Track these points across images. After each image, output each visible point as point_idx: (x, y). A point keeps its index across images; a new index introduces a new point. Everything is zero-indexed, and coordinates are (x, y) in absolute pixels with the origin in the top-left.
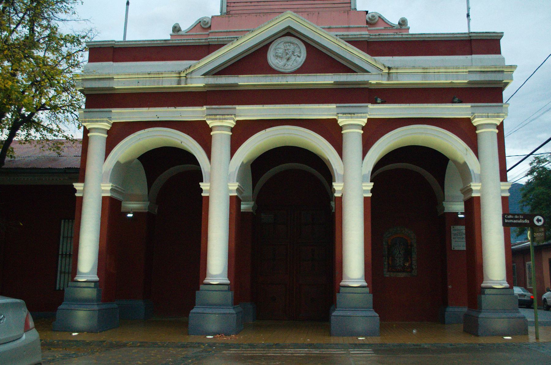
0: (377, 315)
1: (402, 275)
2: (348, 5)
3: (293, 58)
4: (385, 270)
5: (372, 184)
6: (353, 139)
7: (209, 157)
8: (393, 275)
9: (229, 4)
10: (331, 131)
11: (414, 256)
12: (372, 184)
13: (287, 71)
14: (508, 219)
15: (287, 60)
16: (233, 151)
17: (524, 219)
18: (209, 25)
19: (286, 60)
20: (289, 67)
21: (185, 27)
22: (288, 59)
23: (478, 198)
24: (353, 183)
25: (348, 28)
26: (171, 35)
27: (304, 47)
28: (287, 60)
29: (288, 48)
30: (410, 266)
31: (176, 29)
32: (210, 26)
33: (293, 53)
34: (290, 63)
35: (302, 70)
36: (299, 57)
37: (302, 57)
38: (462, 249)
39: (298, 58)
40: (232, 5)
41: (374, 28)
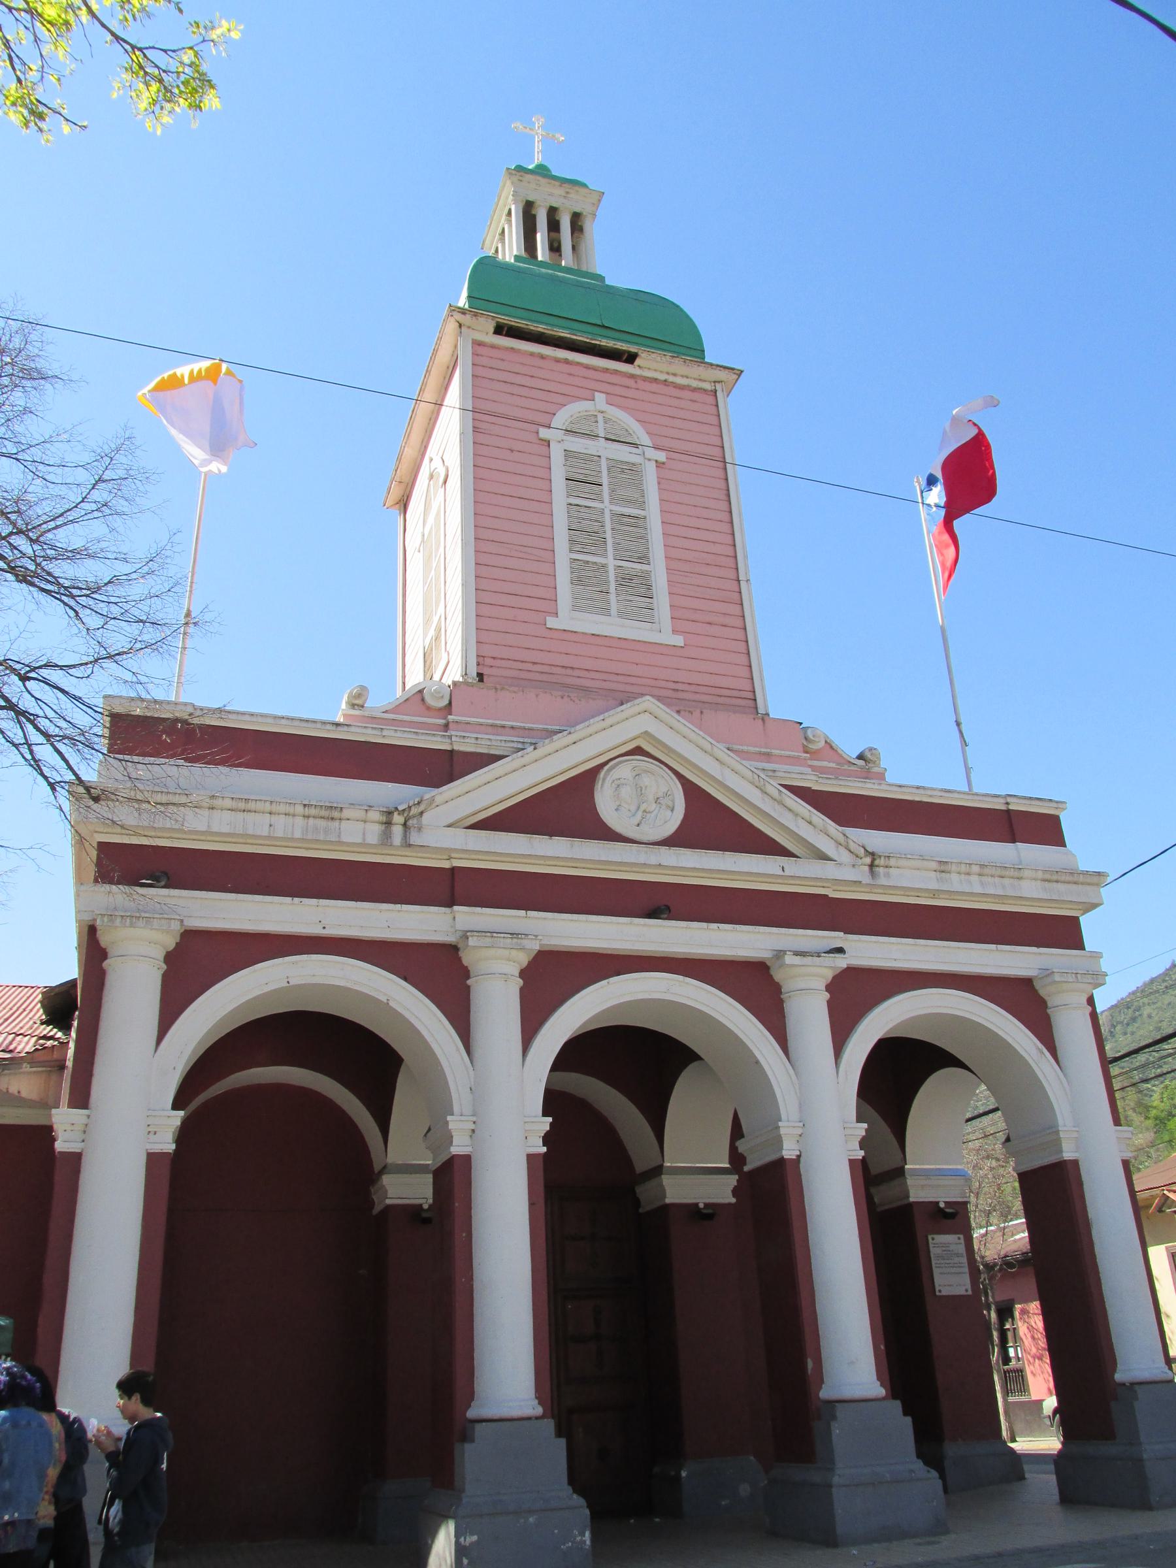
6: (810, 1012)
13: (645, 839)
21: (377, 701)
23: (1075, 1163)
25: (768, 755)
26: (345, 715)
31: (357, 701)
35: (671, 842)
38: (963, 1292)
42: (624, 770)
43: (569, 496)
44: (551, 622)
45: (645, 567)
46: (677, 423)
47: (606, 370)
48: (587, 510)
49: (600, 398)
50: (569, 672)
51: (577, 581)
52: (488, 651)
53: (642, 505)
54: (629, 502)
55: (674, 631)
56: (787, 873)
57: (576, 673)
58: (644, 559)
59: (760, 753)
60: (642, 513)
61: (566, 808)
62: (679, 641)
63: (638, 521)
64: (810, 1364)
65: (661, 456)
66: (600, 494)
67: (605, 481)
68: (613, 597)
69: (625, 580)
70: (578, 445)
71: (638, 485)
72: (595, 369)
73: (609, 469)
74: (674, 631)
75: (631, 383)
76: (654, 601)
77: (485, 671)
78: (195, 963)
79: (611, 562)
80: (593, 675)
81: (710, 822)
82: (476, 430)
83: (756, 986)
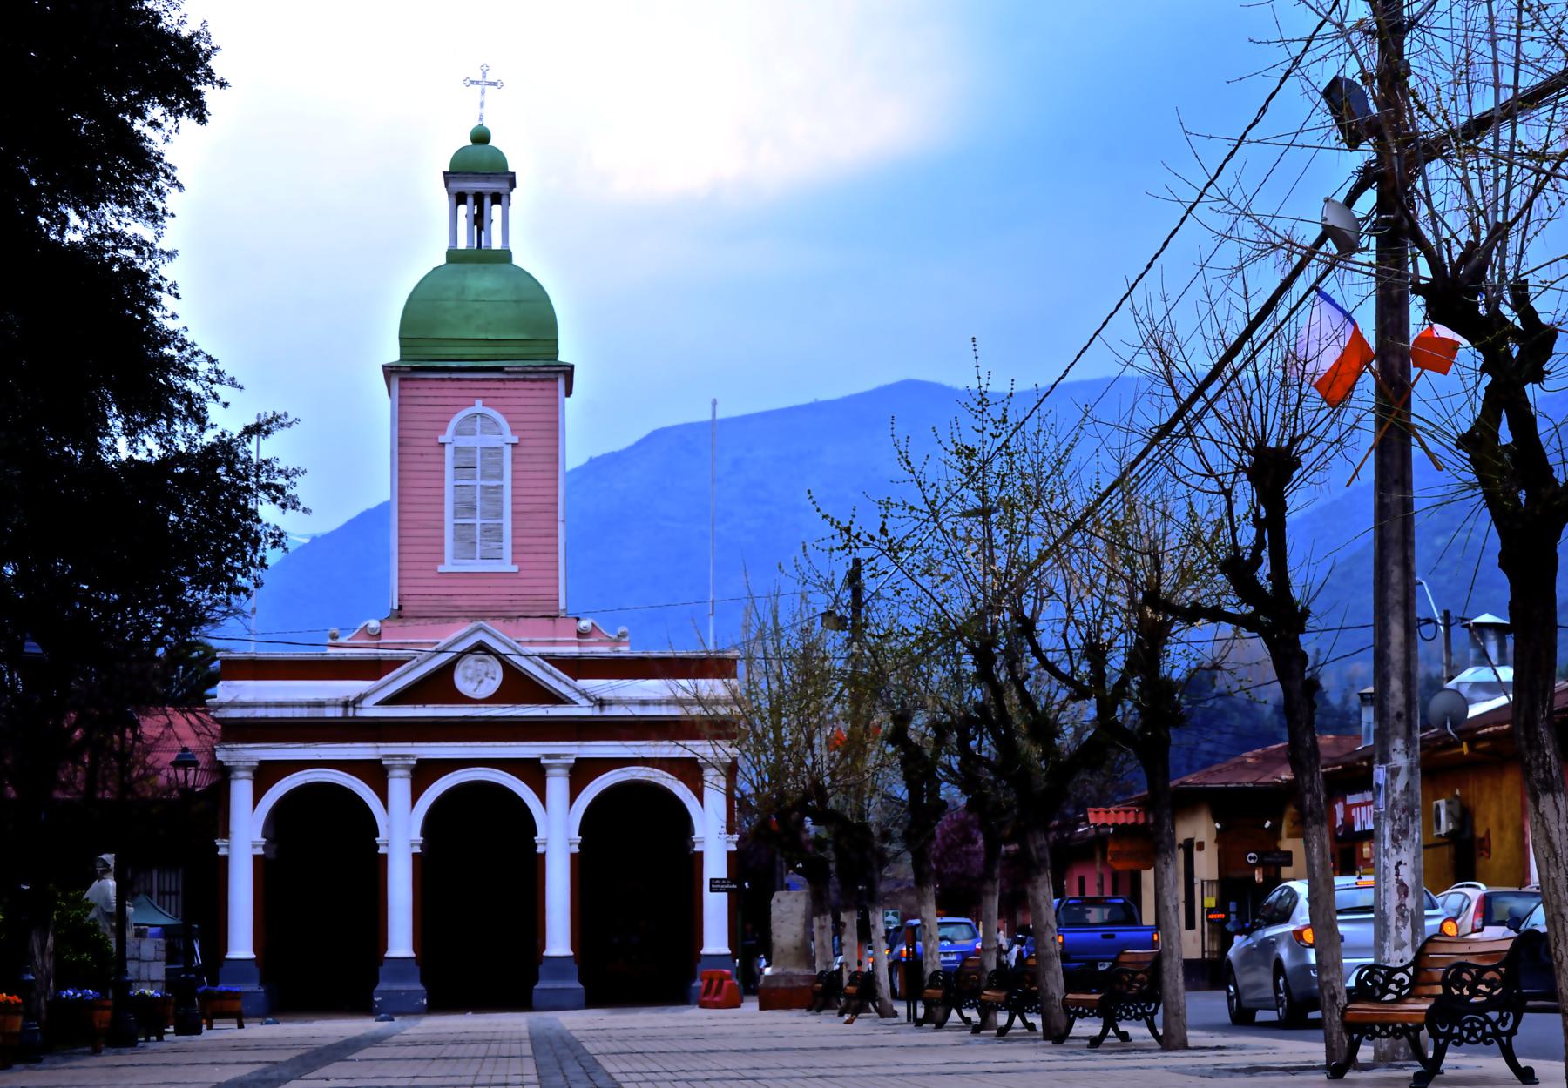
3: (486, 680)
7: (386, 807)
15: (478, 680)
16: (415, 797)
23: (701, 854)
24: (558, 828)
28: (478, 680)
34: (483, 686)
42: (470, 661)
44: (441, 569)
46: (530, 410)
49: (479, 402)
51: (458, 538)
52: (406, 591)
53: (500, 476)
54: (493, 477)
55: (514, 562)
58: (499, 515)
61: (438, 685)
62: (515, 568)
65: (516, 440)
70: (462, 441)
71: (499, 463)
74: (514, 562)
78: (266, 775)
79: (478, 521)
81: (517, 685)
82: (400, 444)
83: (533, 772)
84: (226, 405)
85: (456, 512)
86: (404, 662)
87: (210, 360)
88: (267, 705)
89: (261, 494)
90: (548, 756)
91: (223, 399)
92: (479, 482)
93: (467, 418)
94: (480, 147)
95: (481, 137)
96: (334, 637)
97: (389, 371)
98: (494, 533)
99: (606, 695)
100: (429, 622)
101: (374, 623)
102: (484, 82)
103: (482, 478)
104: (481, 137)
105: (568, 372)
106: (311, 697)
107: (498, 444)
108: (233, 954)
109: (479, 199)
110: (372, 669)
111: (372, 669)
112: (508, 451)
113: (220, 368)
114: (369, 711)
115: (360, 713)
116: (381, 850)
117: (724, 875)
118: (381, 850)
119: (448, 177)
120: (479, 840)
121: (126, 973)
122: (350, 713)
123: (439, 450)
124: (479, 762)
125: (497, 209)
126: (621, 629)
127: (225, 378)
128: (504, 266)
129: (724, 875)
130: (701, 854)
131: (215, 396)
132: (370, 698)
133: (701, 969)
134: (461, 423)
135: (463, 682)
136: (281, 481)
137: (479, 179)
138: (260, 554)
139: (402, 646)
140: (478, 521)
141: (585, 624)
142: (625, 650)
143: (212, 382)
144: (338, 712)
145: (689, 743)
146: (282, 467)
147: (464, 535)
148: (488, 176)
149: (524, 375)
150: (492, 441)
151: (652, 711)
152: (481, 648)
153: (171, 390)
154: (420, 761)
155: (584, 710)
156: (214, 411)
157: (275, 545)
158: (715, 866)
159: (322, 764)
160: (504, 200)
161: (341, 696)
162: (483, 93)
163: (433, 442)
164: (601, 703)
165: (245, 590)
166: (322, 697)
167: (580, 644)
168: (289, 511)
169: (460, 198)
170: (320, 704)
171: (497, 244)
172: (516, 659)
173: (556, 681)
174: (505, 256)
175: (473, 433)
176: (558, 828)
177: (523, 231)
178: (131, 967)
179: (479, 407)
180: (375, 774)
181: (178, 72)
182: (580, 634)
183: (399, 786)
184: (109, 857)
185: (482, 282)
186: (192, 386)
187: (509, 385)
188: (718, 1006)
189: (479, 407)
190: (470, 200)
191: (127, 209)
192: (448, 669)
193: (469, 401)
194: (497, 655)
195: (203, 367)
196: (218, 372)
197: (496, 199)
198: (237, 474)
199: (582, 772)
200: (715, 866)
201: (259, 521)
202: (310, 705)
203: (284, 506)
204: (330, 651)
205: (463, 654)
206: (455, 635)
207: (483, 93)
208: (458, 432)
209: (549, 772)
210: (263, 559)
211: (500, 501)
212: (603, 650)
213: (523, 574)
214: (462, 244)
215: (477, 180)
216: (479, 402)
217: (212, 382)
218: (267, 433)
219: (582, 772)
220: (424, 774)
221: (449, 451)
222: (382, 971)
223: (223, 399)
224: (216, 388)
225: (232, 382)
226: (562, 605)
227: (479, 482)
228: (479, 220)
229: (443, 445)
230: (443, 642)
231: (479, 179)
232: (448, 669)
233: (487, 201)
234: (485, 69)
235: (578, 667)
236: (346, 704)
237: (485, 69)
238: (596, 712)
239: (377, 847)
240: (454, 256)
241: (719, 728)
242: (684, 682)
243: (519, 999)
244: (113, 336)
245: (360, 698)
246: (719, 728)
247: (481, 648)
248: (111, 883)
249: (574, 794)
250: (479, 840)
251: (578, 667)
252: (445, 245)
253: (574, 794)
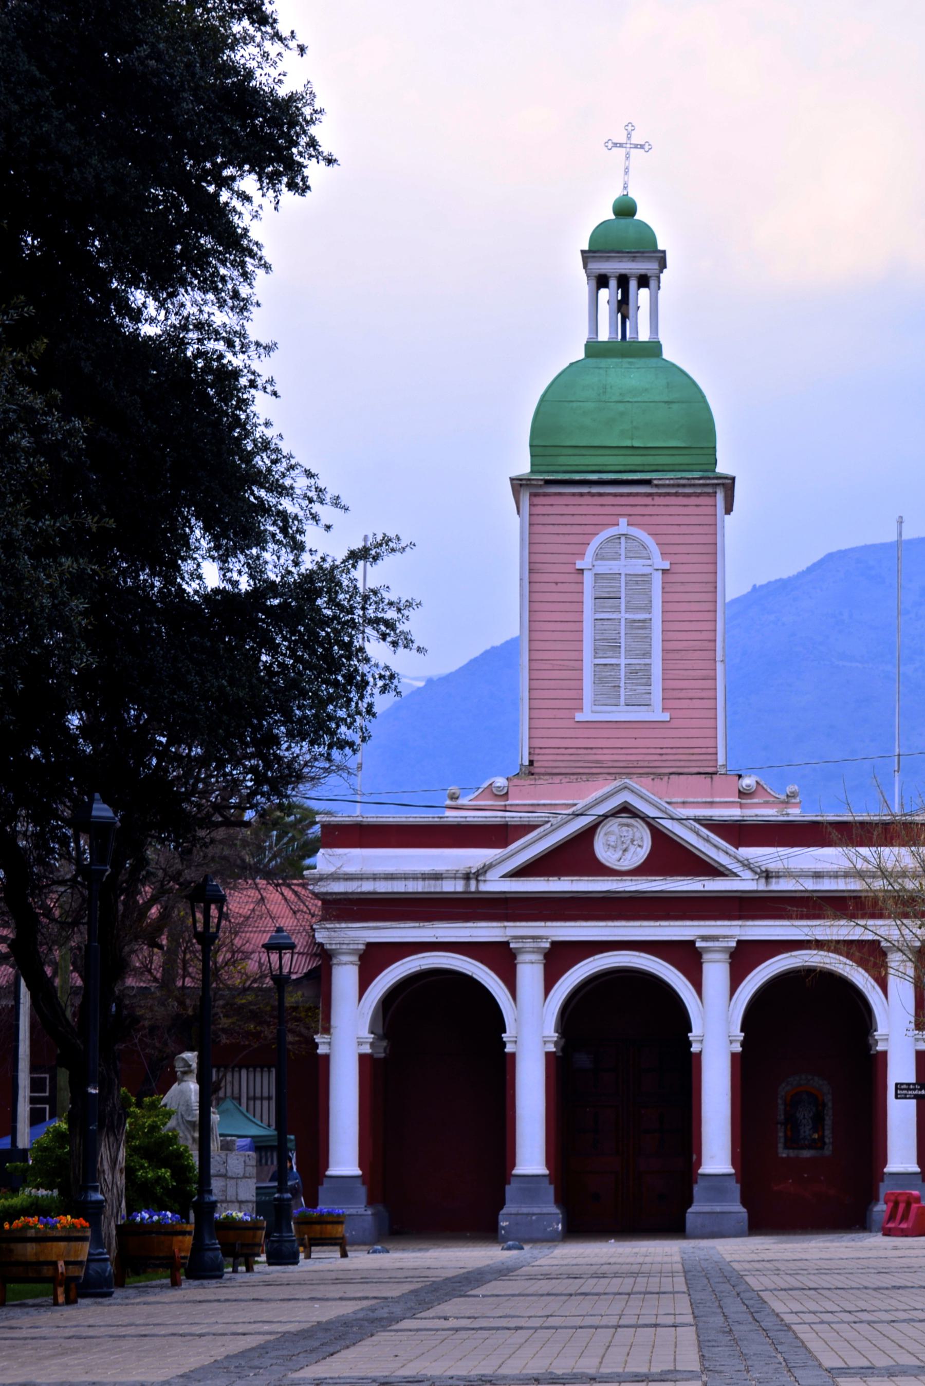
0: (745, 1210)
1: (806, 1154)
2: (713, 757)
3: (632, 849)
4: (781, 1145)
5: (743, 1034)
8: (792, 1153)
9: (532, 751)
10: (687, 957)
11: (828, 1121)
12: (743, 1034)
14: (902, 1089)
17: (920, 1090)
18: (505, 791)
19: (621, 852)
20: (626, 863)
22: (625, 850)
23: (884, 1054)
27: (648, 832)
29: (625, 834)
30: (822, 1138)
32: (507, 793)
33: (632, 841)
34: (628, 855)
36: (640, 846)
37: (644, 848)
39: (639, 849)
40: (537, 751)
41: (749, 801)
42: (613, 825)
43: (596, 612)
44: (579, 717)
45: (647, 661)
46: (684, 529)
47: (630, 495)
48: (609, 622)
49: (623, 521)
50: (589, 751)
51: (599, 680)
52: (537, 743)
53: (648, 608)
55: (664, 709)
56: (706, 889)
57: (594, 751)
58: (647, 654)
59: (706, 802)
60: (646, 616)
62: (666, 717)
63: (646, 624)
64: (694, 1157)
66: (619, 607)
67: (623, 596)
68: (622, 690)
69: (633, 672)
70: (603, 567)
71: (648, 595)
72: (622, 495)
73: (626, 583)
74: (664, 709)
75: (648, 500)
76: (652, 687)
77: (535, 758)
78: (373, 959)
79: (623, 661)
80: (605, 751)
81: (668, 855)
82: (531, 571)
84: (328, 528)
85: (596, 651)
86: (533, 827)
87: (309, 474)
88: (375, 877)
89: (369, 630)
90: (704, 938)
91: (324, 521)
92: (624, 615)
93: (609, 540)
94: (624, 221)
95: (625, 209)
96: (453, 797)
97: (518, 484)
98: (640, 675)
99: (772, 867)
100: (565, 780)
101: (500, 782)
102: (628, 145)
103: (626, 612)
104: (625, 209)
105: (728, 485)
106: (426, 868)
107: (647, 570)
108: (334, 1170)
109: (623, 281)
110: (497, 835)
111: (497, 835)
112: (657, 578)
113: (322, 485)
114: (495, 884)
115: (484, 887)
116: (509, 1049)
117: (914, 1081)
118: (509, 1049)
119: (587, 256)
120: (624, 1037)
121: (210, 1192)
122: (473, 887)
123: (574, 577)
124: (623, 946)
125: (644, 293)
126: (790, 789)
127: (327, 498)
128: (653, 361)
129: (914, 1081)
130: (884, 1054)
131: (315, 517)
132: (496, 870)
133: (884, 1189)
134: (601, 547)
135: (603, 851)
136: (391, 614)
137: (624, 259)
138: (367, 700)
139: (532, 808)
140: (623, 661)
141: (748, 782)
142: (795, 814)
143: (311, 501)
144: (458, 886)
145: (871, 922)
146: (394, 599)
147: (606, 677)
148: (634, 255)
149: (677, 490)
150: (638, 566)
151: (827, 885)
152: (626, 810)
153: (262, 508)
154: (554, 944)
155: (746, 883)
156: (312, 536)
157: (384, 689)
158: (901, 1069)
159: (439, 947)
160: (653, 283)
161: (462, 868)
162: (627, 158)
163: (569, 568)
164: (767, 875)
165: (351, 744)
166: (440, 868)
167: (741, 806)
168: (401, 650)
169: (602, 281)
170: (437, 877)
171: (644, 335)
172: (668, 824)
173: (714, 849)
174: (653, 349)
175: (616, 557)
176: (716, 1023)
177: (673, 317)
178: (216, 1185)
179: (623, 526)
180: (502, 958)
181: (272, 136)
182: (742, 794)
183: (530, 972)
184: (191, 1057)
185: (627, 377)
186: (286, 504)
187: (658, 501)
188: (904, 1233)
189: (623, 526)
190: (613, 283)
191: (210, 296)
192: (587, 836)
193: (611, 520)
194: (645, 819)
195: (301, 483)
196: (319, 490)
197: (644, 281)
198: (339, 605)
199: (745, 957)
200: (901, 1069)
201: (367, 660)
202: (425, 877)
203: (395, 644)
204: (449, 813)
205: (606, 817)
206: (597, 796)
207: (627, 158)
208: (598, 557)
209: (706, 957)
210: (370, 706)
211: (648, 639)
212: (770, 814)
213: (675, 723)
214: (604, 335)
215: (620, 260)
216: (623, 521)
217: (311, 501)
218: (376, 558)
219: (745, 957)
220: (559, 957)
221: (588, 578)
222: (510, 1190)
223: (324, 521)
224: (316, 508)
225: (336, 502)
226: (721, 761)
227: (624, 615)
228: (623, 306)
229: (582, 570)
230: (581, 803)
231: (624, 259)
232: (587, 836)
233: (633, 284)
234: (630, 129)
235: (740, 833)
236: (467, 877)
237: (630, 129)
238: (761, 886)
239: (504, 1045)
240: (594, 350)
241: (906, 906)
242: (864, 851)
243: (672, 1225)
244: (193, 444)
245: (485, 869)
246: (906, 906)
247: (626, 810)
248: (192, 1087)
249: (736, 979)
250: (624, 1037)
251: (740, 833)
252: (584, 336)
253: (736, 979)
